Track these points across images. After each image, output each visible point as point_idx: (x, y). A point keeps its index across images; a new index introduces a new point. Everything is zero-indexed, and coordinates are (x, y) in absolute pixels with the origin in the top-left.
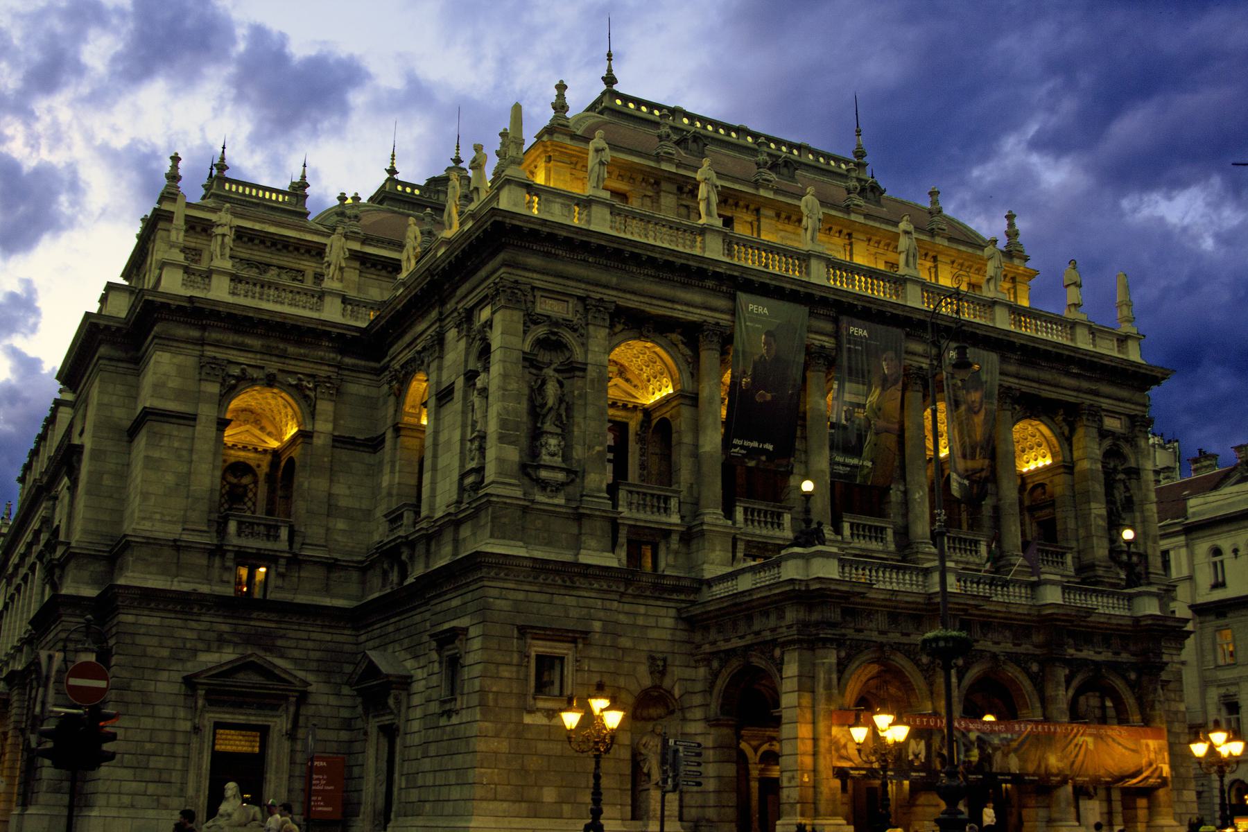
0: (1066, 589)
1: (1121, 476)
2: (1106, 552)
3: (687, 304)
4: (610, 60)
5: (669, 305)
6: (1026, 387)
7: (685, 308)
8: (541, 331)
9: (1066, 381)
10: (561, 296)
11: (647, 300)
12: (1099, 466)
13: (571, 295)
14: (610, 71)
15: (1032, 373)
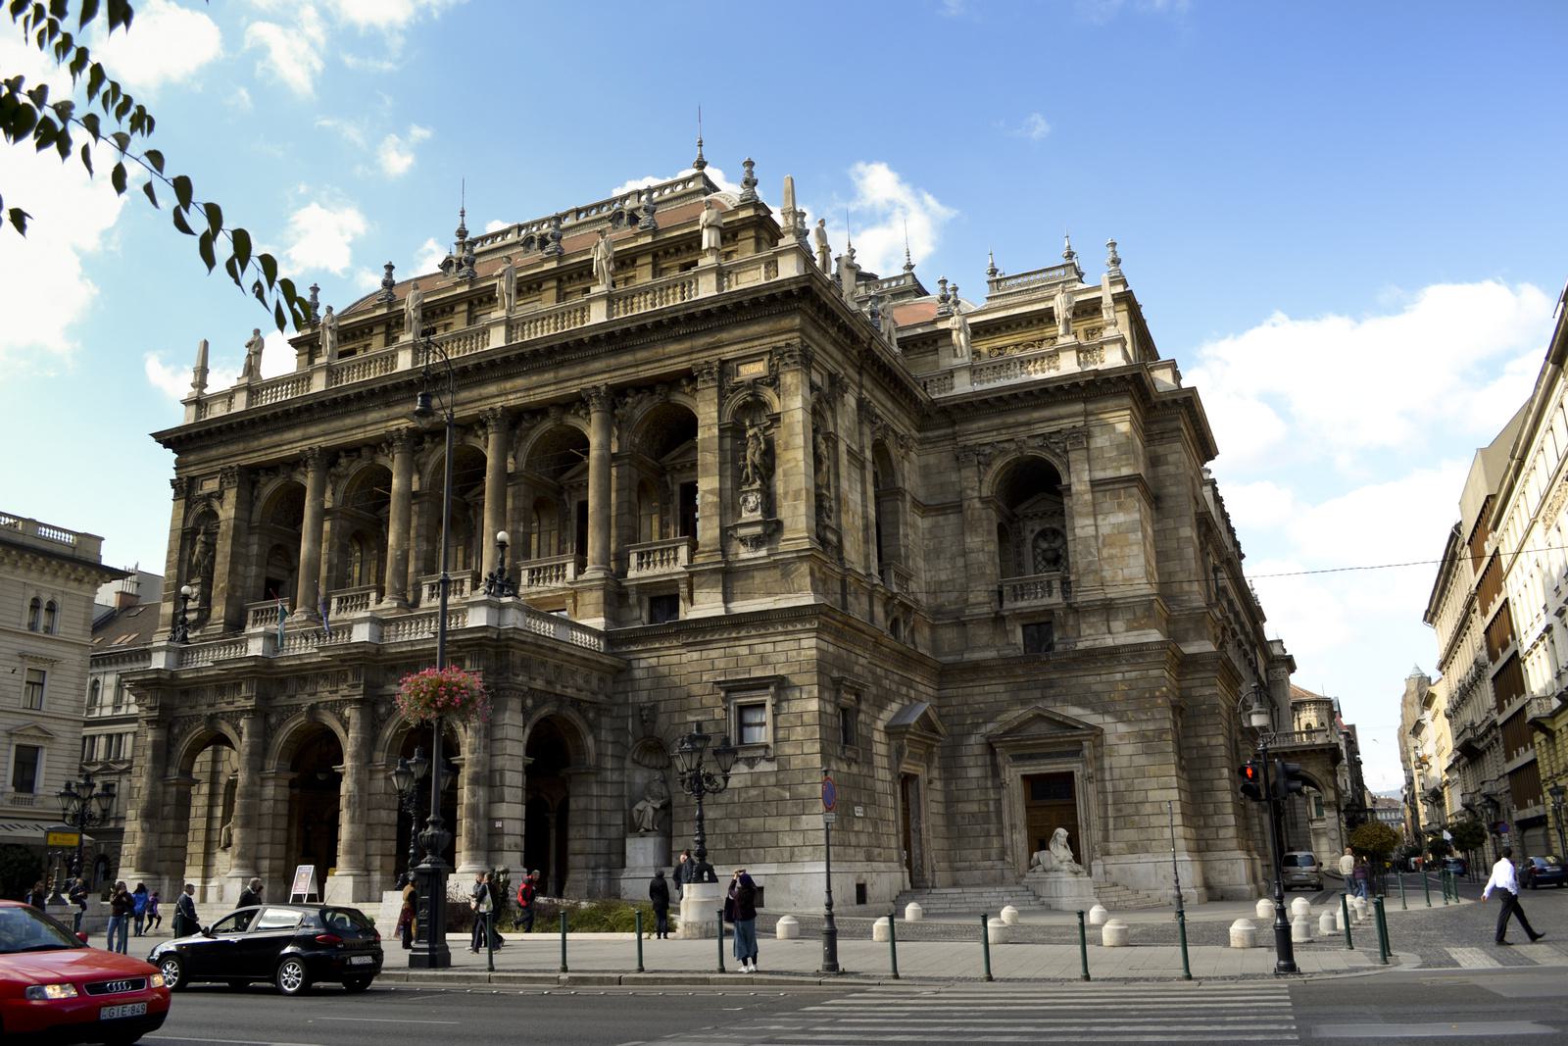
0: (378, 623)
1: (751, 432)
2: (718, 531)
3: (291, 443)
4: (463, 216)
5: (278, 449)
6: (616, 378)
7: (290, 446)
8: (200, 508)
9: (673, 348)
10: (210, 476)
11: (263, 453)
12: (716, 431)
13: (218, 472)
14: (463, 225)
15: (627, 358)
